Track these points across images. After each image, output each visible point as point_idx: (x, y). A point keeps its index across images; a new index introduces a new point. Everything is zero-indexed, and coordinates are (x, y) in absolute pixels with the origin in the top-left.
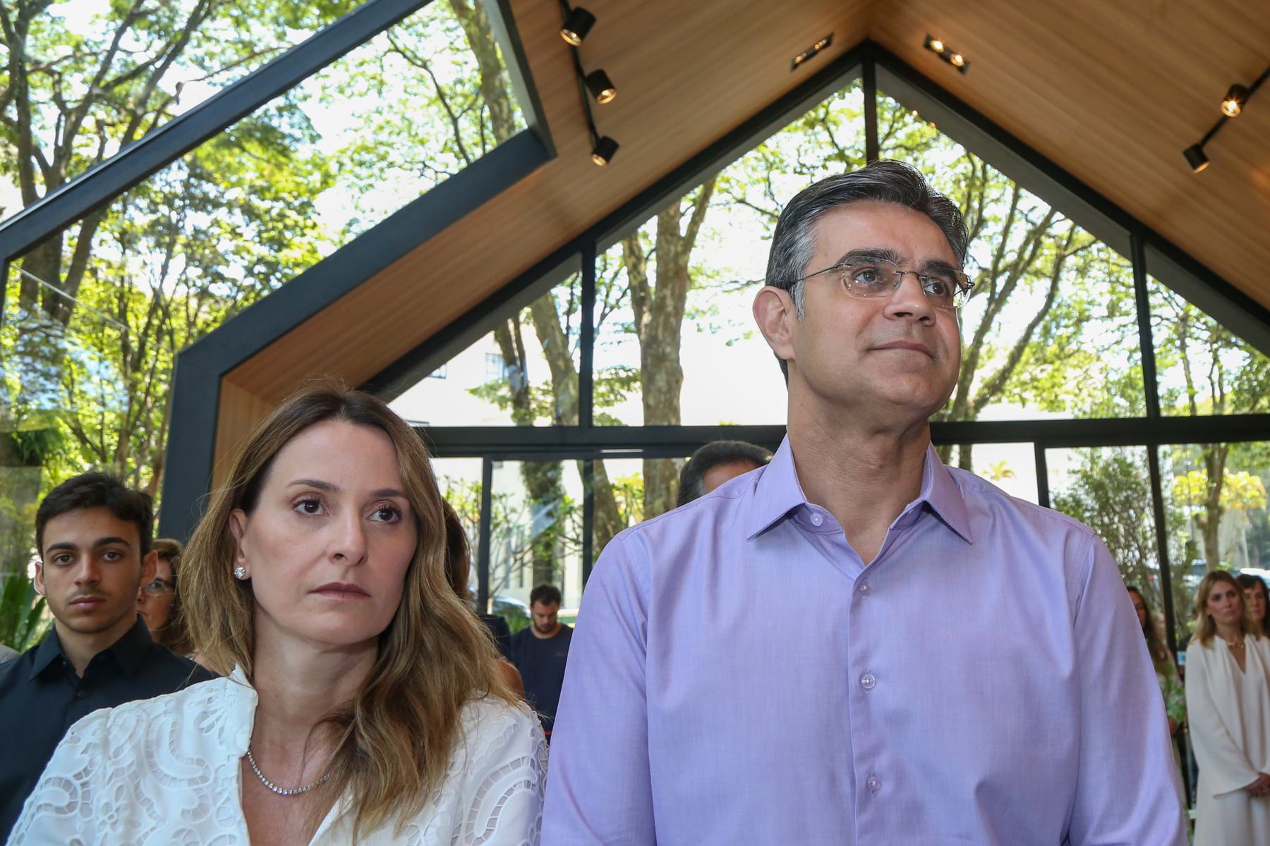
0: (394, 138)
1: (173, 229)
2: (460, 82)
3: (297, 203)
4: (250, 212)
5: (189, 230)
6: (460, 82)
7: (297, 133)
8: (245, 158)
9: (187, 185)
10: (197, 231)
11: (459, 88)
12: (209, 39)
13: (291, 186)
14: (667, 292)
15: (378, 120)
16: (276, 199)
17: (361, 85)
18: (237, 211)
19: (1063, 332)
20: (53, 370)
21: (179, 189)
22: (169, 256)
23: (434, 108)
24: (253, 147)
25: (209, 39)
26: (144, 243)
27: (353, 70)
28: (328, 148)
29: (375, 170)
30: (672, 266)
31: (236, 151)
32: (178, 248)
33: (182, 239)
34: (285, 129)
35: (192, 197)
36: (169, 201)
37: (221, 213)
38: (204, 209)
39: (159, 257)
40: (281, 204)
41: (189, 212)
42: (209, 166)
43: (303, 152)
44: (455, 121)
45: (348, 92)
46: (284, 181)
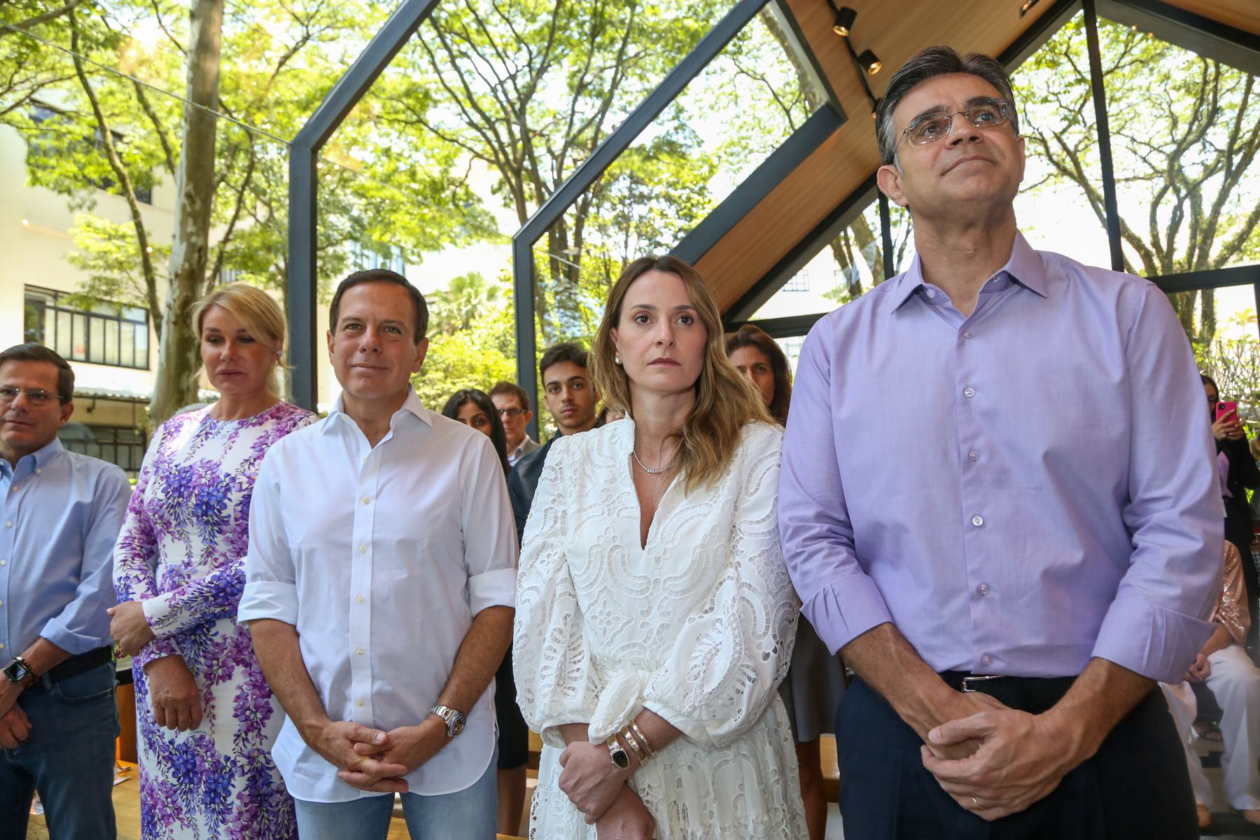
0: (750, 133)
1: (627, 218)
2: (788, 84)
3: (697, 189)
4: (669, 199)
5: (636, 218)
6: (788, 84)
7: (689, 142)
8: (661, 165)
9: (630, 189)
10: (641, 217)
11: (788, 89)
12: (626, 93)
13: (691, 178)
15: (738, 122)
16: (684, 188)
17: (724, 101)
18: (662, 200)
20: (577, 315)
21: (626, 193)
23: (773, 107)
24: (664, 157)
25: (626, 93)
26: (612, 230)
27: (717, 92)
28: (709, 148)
29: (742, 156)
31: (655, 161)
32: (632, 230)
33: (633, 224)
34: (681, 141)
35: (634, 196)
36: (621, 201)
37: (654, 202)
38: (642, 202)
39: (622, 236)
40: (687, 191)
41: (634, 206)
42: (641, 175)
43: (694, 154)
44: (788, 112)
45: (716, 108)
46: (686, 176)
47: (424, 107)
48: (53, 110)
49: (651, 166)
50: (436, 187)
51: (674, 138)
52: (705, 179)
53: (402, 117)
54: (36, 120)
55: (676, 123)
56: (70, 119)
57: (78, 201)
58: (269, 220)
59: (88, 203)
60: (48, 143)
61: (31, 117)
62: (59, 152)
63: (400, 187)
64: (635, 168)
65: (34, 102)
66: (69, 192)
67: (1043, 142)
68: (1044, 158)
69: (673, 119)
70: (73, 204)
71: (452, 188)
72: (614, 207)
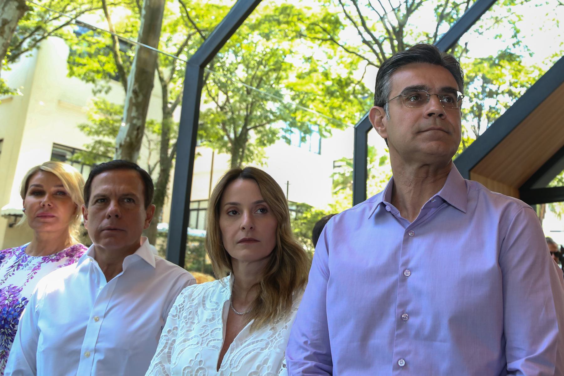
1: (480, 108)
8: (503, 70)
22: (479, 120)
31: (499, 67)
37: (500, 97)
47: (335, 28)
48: (89, 27)
49: (497, 70)
50: (342, 84)
51: (512, 51)
53: (320, 36)
54: (78, 34)
56: (99, 33)
57: (99, 87)
58: (225, 104)
59: (106, 89)
60: (82, 48)
61: (74, 32)
62: (90, 55)
63: (318, 84)
65: (78, 23)
66: (93, 81)
69: (513, 37)
70: (96, 89)
72: (471, 101)
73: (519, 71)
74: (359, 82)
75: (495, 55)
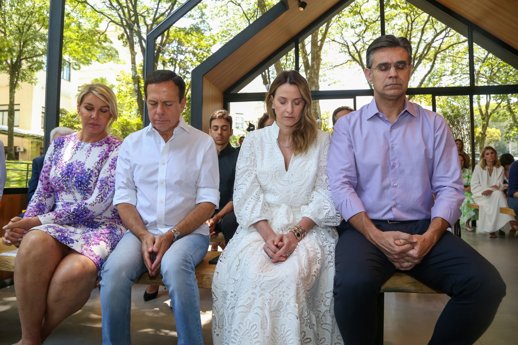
2: (249, 9)
5: (179, 60)
6: (249, 9)
7: (206, 29)
11: (249, 12)
14: (315, 63)
15: (227, 23)
16: (201, 49)
17: (222, 13)
19: (436, 80)
21: (176, 49)
23: (242, 18)
24: (194, 33)
27: (219, 9)
28: (214, 32)
30: (316, 55)
31: (190, 35)
32: (177, 65)
33: (178, 62)
34: (202, 28)
35: (179, 51)
36: (173, 52)
40: (202, 51)
43: (207, 34)
45: (218, 15)
46: (203, 43)
49: (189, 38)
51: (200, 26)
52: (211, 46)
55: (201, 20)
64: (181, 37)
67: (348, 46)
68: (347, 54)
69: (200, 18)
71: (99, 35)
73: (202, 39)
74: (103, 33)
75: (188, 27)
